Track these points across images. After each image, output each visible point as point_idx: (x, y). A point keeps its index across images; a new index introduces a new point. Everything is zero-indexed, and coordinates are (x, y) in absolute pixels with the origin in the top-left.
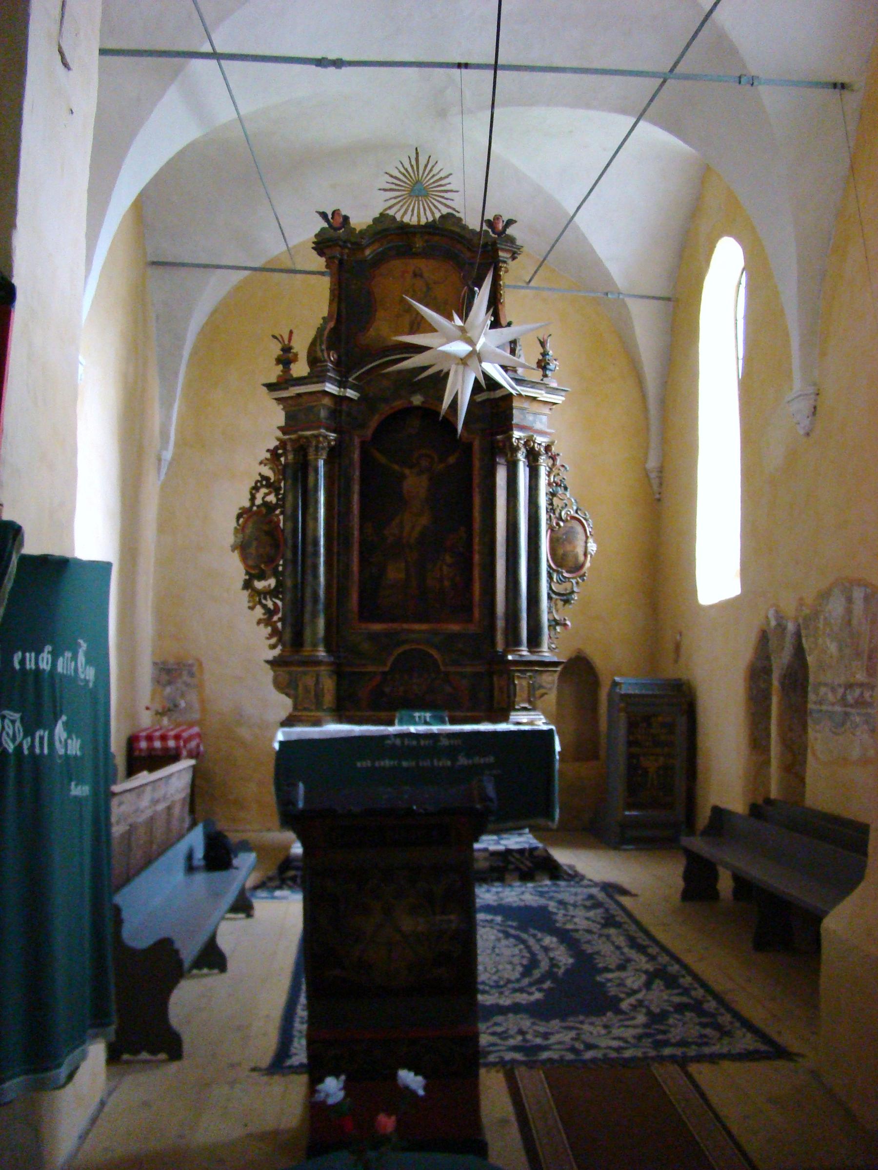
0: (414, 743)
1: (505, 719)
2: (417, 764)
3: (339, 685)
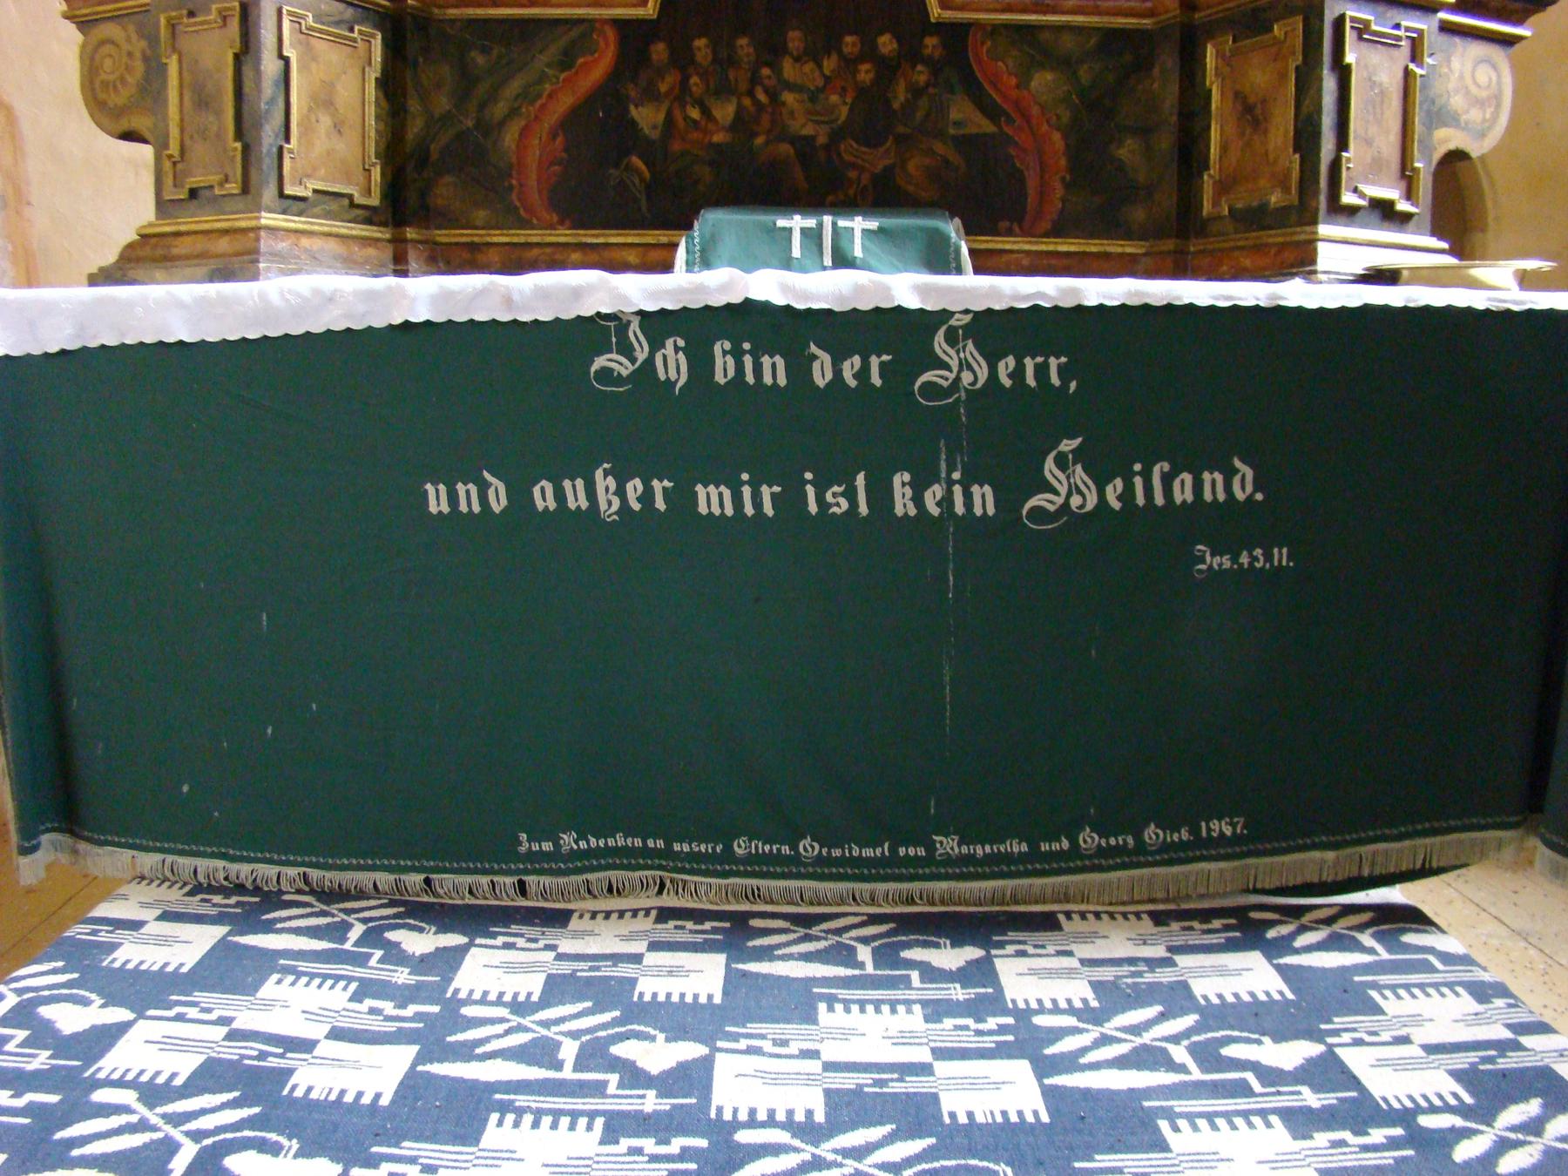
0: (775, 370)
1: (1300, 261)
2: (790, 501)
3: (392, 87)
